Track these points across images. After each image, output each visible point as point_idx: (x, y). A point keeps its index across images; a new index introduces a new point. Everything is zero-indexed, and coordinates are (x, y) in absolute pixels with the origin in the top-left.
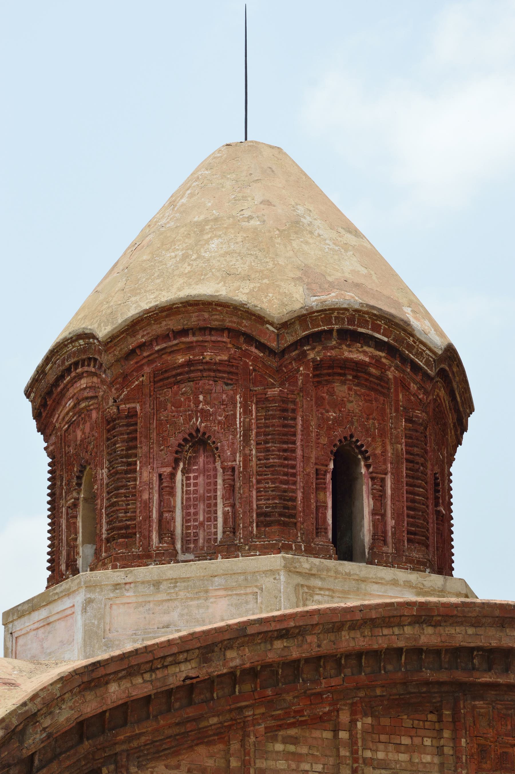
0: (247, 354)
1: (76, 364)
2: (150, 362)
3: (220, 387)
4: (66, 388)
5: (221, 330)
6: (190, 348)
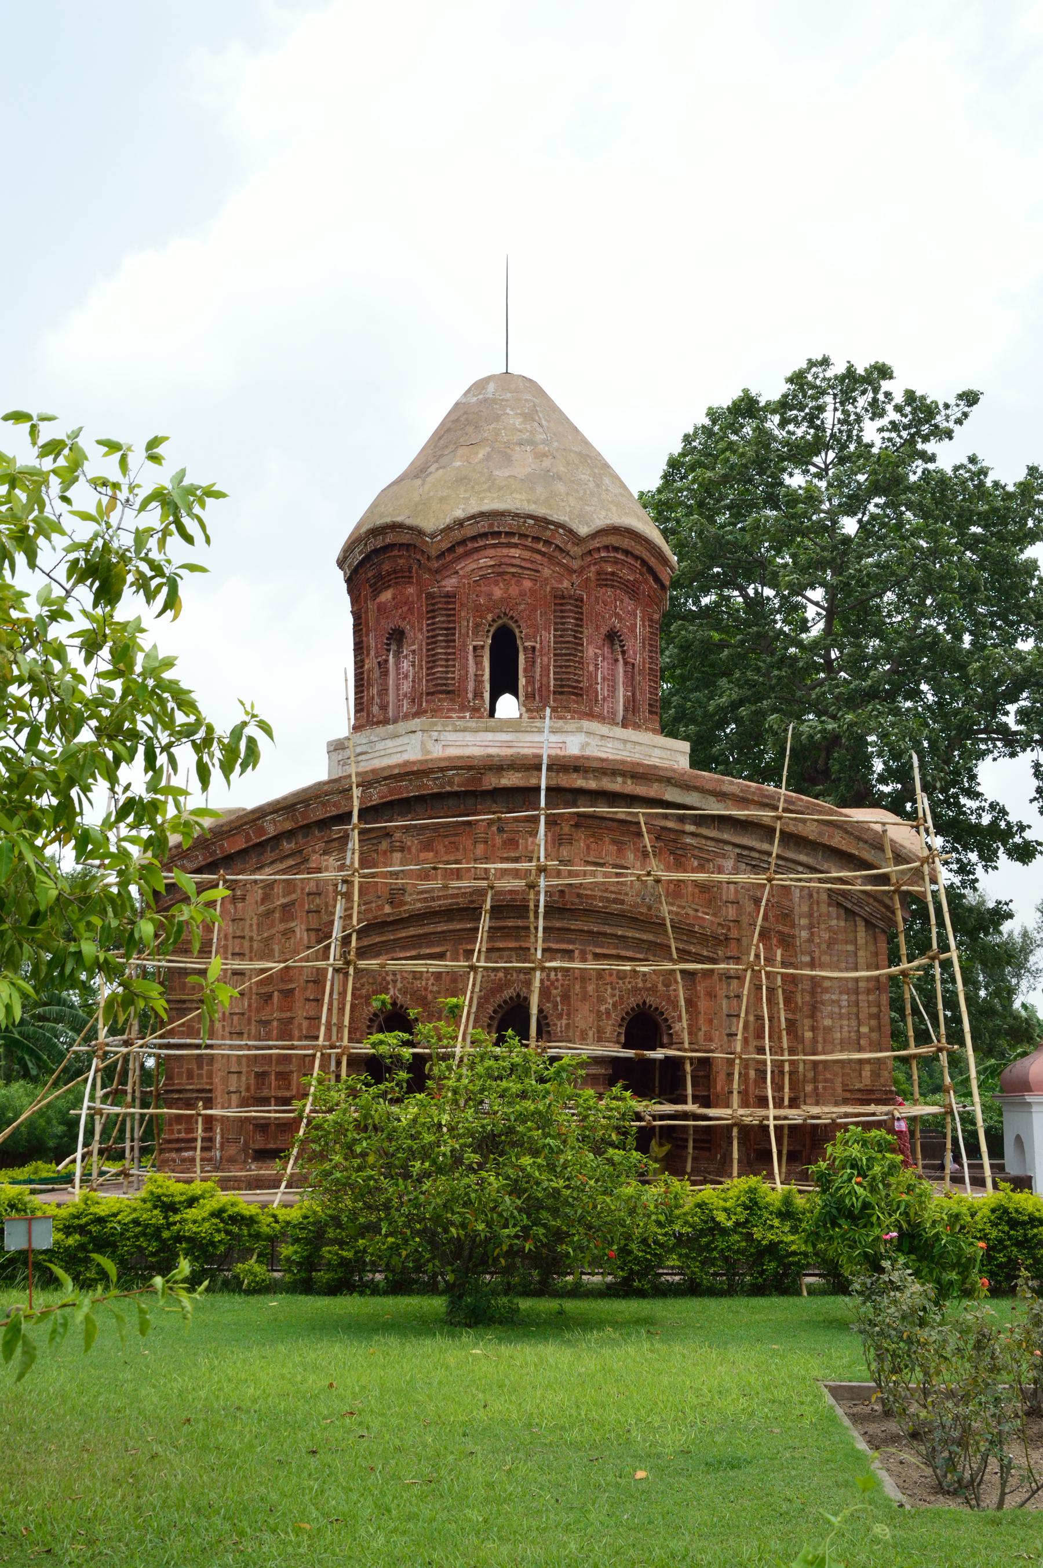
0: (646, 581)
1: (508, 534)
2: (595, 564)
3: (626, 600)
4: (485, 547)
5: (637, 558)
6: (616, 561)
